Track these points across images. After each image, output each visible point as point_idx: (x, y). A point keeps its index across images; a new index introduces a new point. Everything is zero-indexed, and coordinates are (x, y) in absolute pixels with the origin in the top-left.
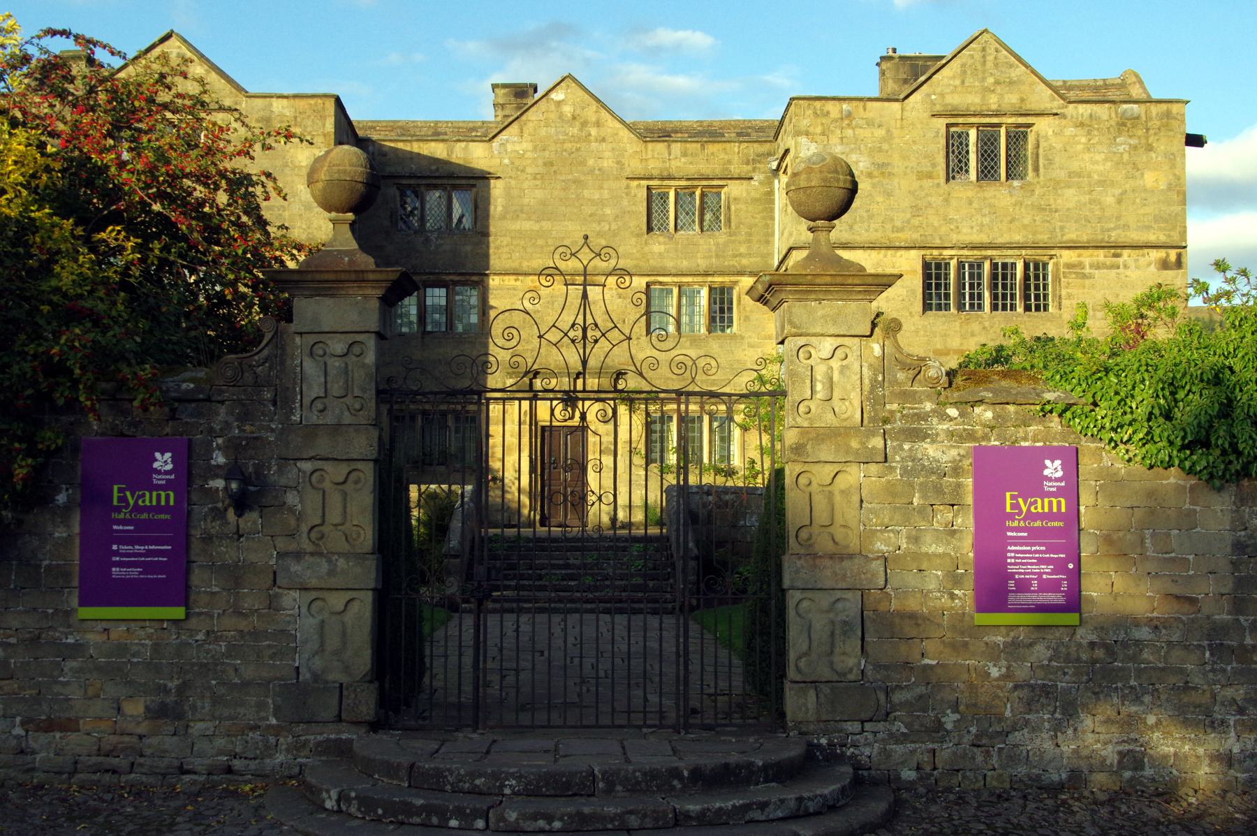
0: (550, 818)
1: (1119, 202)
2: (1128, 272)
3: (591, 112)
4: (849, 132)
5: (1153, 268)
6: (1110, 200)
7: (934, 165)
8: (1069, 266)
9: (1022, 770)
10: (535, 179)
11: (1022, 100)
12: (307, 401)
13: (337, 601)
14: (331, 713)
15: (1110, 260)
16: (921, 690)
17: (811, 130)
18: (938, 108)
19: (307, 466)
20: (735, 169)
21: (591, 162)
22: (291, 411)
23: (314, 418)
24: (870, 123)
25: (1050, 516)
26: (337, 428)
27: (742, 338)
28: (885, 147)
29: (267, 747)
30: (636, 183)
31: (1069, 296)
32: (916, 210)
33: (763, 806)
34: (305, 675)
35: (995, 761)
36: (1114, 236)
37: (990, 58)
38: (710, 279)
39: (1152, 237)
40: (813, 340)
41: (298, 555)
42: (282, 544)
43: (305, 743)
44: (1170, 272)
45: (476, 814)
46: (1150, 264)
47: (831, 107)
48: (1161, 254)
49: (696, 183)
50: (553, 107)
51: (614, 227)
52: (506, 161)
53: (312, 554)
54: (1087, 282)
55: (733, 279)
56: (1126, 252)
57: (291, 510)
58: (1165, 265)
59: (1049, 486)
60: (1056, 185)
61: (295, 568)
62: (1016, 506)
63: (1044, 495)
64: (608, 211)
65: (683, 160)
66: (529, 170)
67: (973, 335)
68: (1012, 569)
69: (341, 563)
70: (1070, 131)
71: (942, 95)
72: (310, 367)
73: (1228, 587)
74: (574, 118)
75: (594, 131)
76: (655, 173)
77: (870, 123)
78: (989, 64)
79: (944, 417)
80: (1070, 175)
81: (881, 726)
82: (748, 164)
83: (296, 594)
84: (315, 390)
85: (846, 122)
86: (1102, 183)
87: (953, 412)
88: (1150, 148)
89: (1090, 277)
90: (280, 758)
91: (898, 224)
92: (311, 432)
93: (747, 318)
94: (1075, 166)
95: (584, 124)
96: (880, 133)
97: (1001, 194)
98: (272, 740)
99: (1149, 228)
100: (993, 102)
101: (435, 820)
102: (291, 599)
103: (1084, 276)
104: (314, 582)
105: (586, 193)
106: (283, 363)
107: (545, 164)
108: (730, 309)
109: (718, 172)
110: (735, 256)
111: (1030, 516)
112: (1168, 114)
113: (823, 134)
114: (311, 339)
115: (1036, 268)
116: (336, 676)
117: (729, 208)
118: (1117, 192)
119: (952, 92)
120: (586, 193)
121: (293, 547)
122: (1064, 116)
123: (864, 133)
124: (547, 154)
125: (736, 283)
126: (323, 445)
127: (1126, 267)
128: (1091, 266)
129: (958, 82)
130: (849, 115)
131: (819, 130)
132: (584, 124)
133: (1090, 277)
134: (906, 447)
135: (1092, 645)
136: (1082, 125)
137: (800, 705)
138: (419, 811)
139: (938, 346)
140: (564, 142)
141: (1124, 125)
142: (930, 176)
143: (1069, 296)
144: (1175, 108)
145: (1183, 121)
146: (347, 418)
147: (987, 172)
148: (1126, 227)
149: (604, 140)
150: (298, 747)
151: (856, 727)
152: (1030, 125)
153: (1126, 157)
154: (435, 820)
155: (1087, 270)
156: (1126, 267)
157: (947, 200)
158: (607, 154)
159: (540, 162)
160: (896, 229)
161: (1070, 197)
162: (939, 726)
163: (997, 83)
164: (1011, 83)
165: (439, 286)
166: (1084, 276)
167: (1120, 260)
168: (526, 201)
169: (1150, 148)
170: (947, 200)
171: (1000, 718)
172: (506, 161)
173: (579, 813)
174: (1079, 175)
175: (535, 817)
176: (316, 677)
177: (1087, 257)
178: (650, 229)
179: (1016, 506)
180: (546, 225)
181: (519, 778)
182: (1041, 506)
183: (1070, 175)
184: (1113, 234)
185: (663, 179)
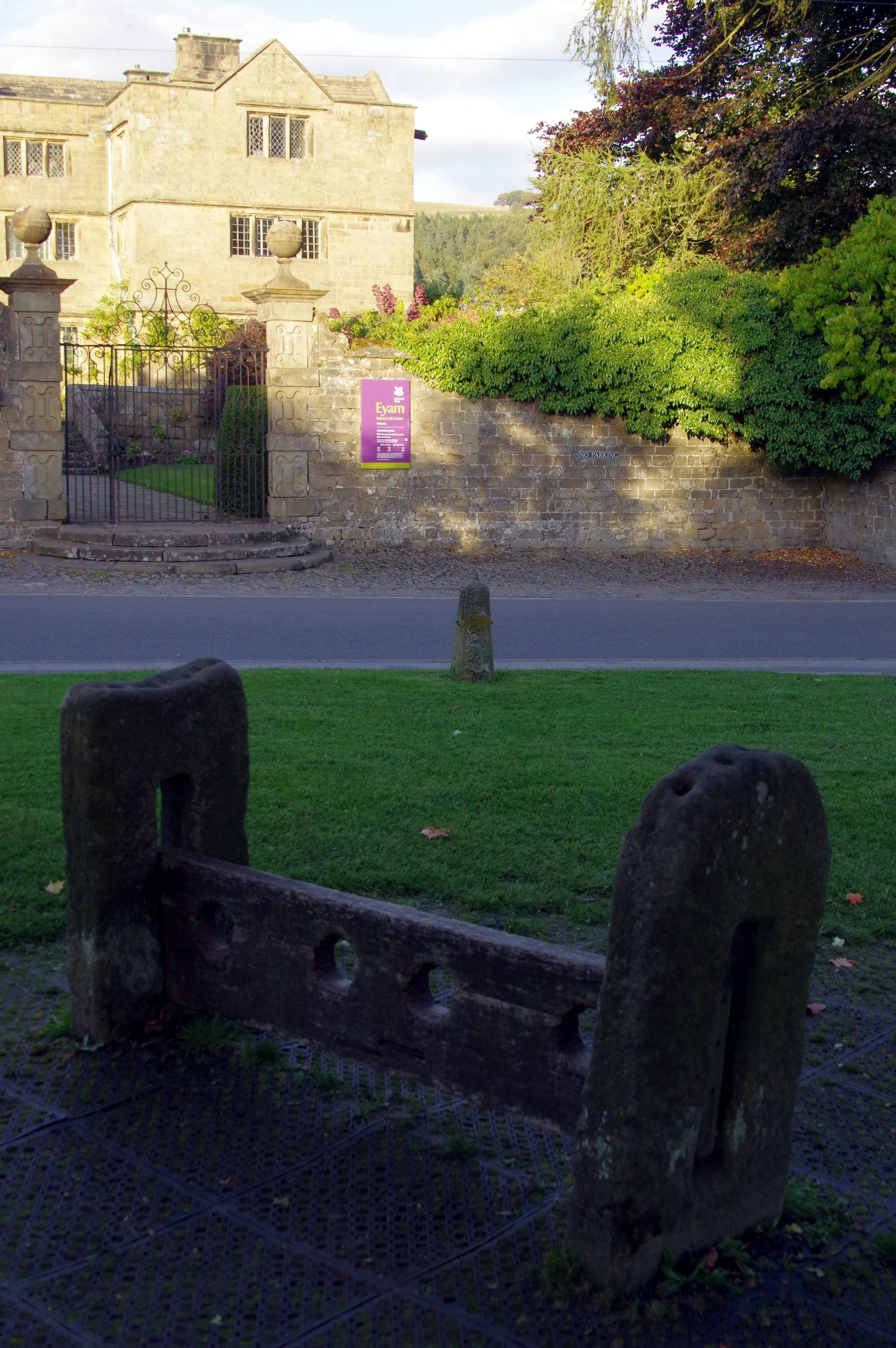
0: (193, 555)
1: (369, 180)
4: (175, 113)
5: (391, 231)
7: (238, 143)
8: (334, 226)
9: (382, 539)
11: (302, 97)
12: (23, 349)
13: (43, 457)
14: (42, 516)
15: (362, 223)
16: (336, 501)
17: (146, 108)
18: (241, 99)
19: (25, 385)
20: (75, 127)
22: (14, 355)
23: (27, 359)
24: (191, 106)
25: (397, 415)
26: (40, 364)
27: (83, 265)
28: (202, 126)
29: (10, 533)
31: (334, 248)
33: (283, 550)
34: (28, 496)
35: (370, 535)
36: (366, 205)
37: (279, 62)
39: (391, 208)
40: (284, 323)
41: (22, 432)
42: (13, 426)
43: (29, 532)
44: (401, 234)
45: (157, 555)
48: (396, 220)
49: (43, 136)
53: (30, 432)
56: (372, 217)
57: (17, 408)
58: (399, 229)
59: (396, 400)
61: (21, 439)
62: (381, 410)
63: (394, 404)
67: (266, 274)
68: (379, 441)
69: (46, 436)
70: (336, 123)
71: (244, 89)
72: (22, 329)
73: (477, 450)
76: (10, 126)
77: (191, 106)
78: (278, 67)
79: (347, 364)
81: (316, 519)
82: (84, 123)
83: (21, 453)
84: (28, 344)
85: (173, 104)
87: (351, 361)
88: (390, 141)
89: (348, 234)
90: (17, 539)
92: (27, 366)
93: (86, 250)
97: (286, 167)
98: (12, 529)
100: (281, 97)
101: (136, 558)
102: (19, 456)
103: (344, 234)
104: (31, 447)
106: (8, 328)
108: (73, 241)
109: (61, 128)
110: (76, 198)
111: (388, 415)
112: (403, 116)
113: (156, 112)
114: (24, 315)
115: (311, 226)
116: (44, 496)
121: (18, 428)
122: (331, 112)
125: (77, 220)
126: (33, 374)
127: (372, 228)
129: (255, 79)
130: (175, 99)
131: (152, 109)
133: (348, 234)
134: (329, 379)
135: (415, 478)
136: (343, 119)
137: (275, 508)
138: (127, 555)
141: (373, 121)
142: (235, 151)
143: (334, 248)
144: (408, 111)
145: (413, 122)
146: (45, 359)
147: (276, 151)
150: (26, 533)
151: (305, 519)
152: (307, 117)
153: (374, 146)
154: (136, 558)
155: (346, 230)
156: (372, 228)
157: (247, 171)
162: (344, 519)
163: (284, 82)
164: (294, 83)
166: (344, 234)
167: (369, 223)
169: (390, 141)
170: (247, 171)
171: (373, 514)
173: (206, 553)
175: (186, 555)
176: (34, 497)
177: (346, 220)
178: (6, 172)
179: (381, 410)
181: (172, 538)
182: (393, 410)
184: (364, 203)
185: (16, 131)
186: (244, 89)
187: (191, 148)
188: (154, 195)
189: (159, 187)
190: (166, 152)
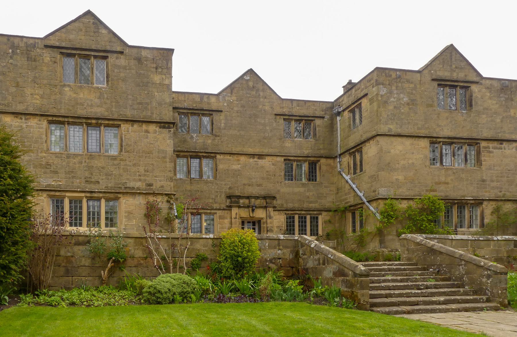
1: (502, 121)
2: (506, 151)
4: (400, 85)
6: (498, 120)
7: (433, 102)
8: (485, 148)
10: (237, 113)
11: (466, 76)
15: (499, 146)
17: (385, 82)
18: (434, 77)
21: (260, 107)
24: (408, 81)
28: (414, 92)
30: (278, 117)
36: (500, 136)
37: (453, 57)
38: (309, 159)
46: (513, 148)
49: (303, 118)
50: (244, 82)
51: (270, 135)
52: (225, 104)
54: (491, 154)
55: (318, 159)
56: (504, 143)
64: (268, 128)
65: (297, 108)
66: (235, 109)
71: (436, 71)
74: (253, 87)
75: (261, 94)
77: (408, 81)
78: (453, 60)
80: (484, 109)
86: (496, 113)
91: (420, 126)
95: (258, 90)
96: (412, 86)
99: (512, 133)
103: (490, 152)
105: (258, 120)
107: (241, 106)
113: (389, 85)
117: (315, 129)
119: (439, 70)
120: (258, 120)
122: (481, 84)
124: (242, 102)
125: (319, 161)
127: (505, 149)
128: (492, 148)
129: (441, 66)
130: (400, 77)
131: (387, 83)
132: (258, 90)
136: (488, 88)
139: (437, 181)
140: (249, 97)
141: (503, 89)
142: (432, 106)
143: (485, 160)
149: (265, 98)
153: (504, 102)
155: (491, 150)
156: (505, 149)
157: (438, 117)
158: (267, 104)
159: (240, 105)
160: (419, 128)
164: (461, 68)
165: (196, 158)
166: (490, 152)
167: (503, 146)
168: (234, 121)
172: (225, 104)
177: (491, 145)
180: (243, 133)
183: (484, 109)
186: (436, 71)
188: (389, 131)
189: (391, 127)
190: (395, 107)
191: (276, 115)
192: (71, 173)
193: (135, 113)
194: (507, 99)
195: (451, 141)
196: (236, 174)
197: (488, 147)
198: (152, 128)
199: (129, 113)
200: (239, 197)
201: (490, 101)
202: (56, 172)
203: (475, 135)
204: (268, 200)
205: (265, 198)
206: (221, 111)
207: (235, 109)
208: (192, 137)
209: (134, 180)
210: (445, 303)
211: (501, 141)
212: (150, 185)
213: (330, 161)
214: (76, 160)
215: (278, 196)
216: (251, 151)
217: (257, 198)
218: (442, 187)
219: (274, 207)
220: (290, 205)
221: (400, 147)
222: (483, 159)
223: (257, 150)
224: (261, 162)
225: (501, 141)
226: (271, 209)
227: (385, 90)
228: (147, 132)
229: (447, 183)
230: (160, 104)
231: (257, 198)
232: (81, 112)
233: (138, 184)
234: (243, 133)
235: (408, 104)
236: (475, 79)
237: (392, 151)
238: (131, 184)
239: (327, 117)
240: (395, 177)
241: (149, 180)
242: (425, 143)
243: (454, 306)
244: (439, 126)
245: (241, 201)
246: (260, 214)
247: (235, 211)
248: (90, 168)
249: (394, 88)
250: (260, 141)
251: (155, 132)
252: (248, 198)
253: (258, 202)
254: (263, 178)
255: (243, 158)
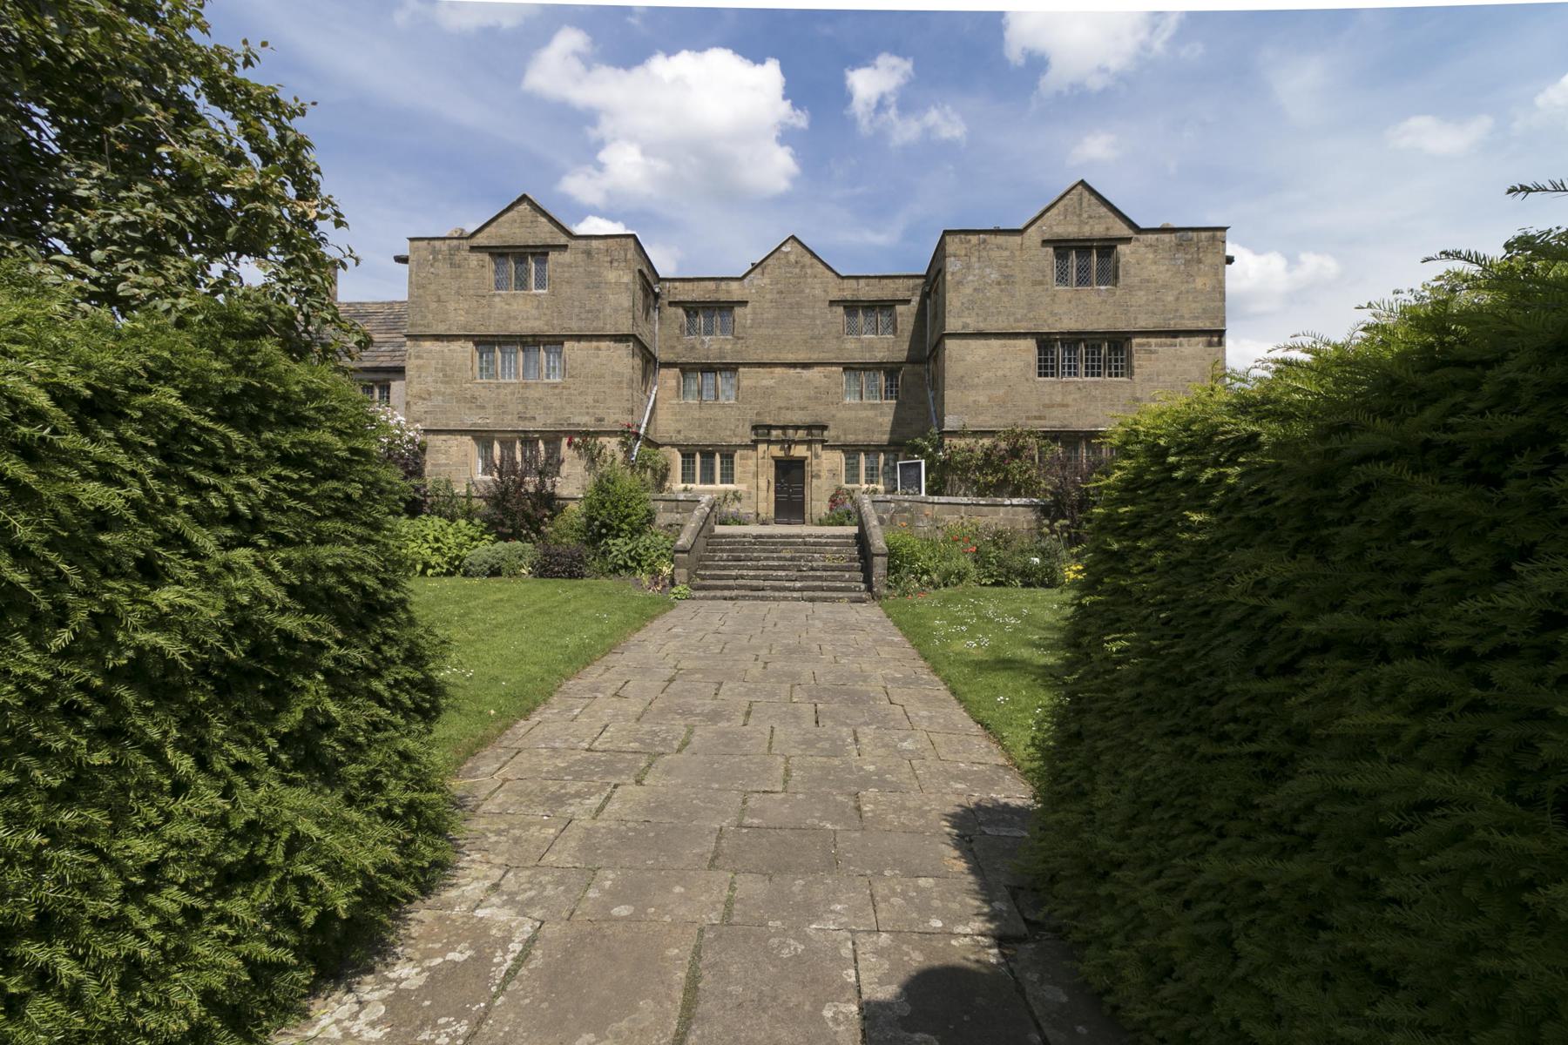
1: (1177, 299)
3: (807, 259)
4: (984, 254)
6: (1170, 298)
8: (1139, 345)
24: (999, 247)
31: (1140, 366)
32: (1031, 306)
36: (1173, 325)
47: (974, 239)
58: (1210, 344)
60: (1130, 289)
70: (1143, 250)
77: (999, 247)
86: (1164, 286)
88: (1199, 261)
94: (1145, 275)
96: (1007, 253)
99: (1197, 318)
103: (1151, 352)
112: (1214, 238)
118: (1176, 292)
123: (995, 254)
142: (1041, 283)
143: (1140, 366)
144: (1219, 234)
148: (1182, 317)
160: (1017, 321)
161: (1141, 297)
166: (1151, 352)
169: (1199, 261)
174: (1148, 281)
177: (1153, 341)
180: (779, 332)
187: (999, 283)
191: (832, 303)
192: (501, 407)
193: (583, 324)
194: (1187, 263)
195: (1072, 340)
196: (767, 392)
197: (1149, 344)
198: (604, 344)
199: (575, 327)
200: (770, 427)
201: (1154, 268)
202: (483, 407)
203: (1122, 326)
204: (815, 431)
205: (809, 428)
206: (746, 302)
207: (768, 296)
208: (703, 342)
209: (580, 414)
210: (800, 590)
211: (1175, 334)
212: (601, 420)
213: (918, 368)
214: (508, 390)
215: (831, 424)
216: (791, 358)
217: (797, 428)
218: (1057, 412)
219: (823, 441)
220: (851, 439)
221: (983, 352)
222: (1135, 363)
223: (802, 357)
224: (806, 373)
225: (1175, 334)
226: (819, 447)
227: (959, 264)
228: (598, 349)
229: (1067, 406)
230: (616, 310)
231: (797, 428)
232: (515, 328)
233: (585, 419)
234: (779, 332)
235: (999, 283)
236: (1126, 232)
237: (968, 358)
238: (576, 420)
239: (916, 300)
240: (971, 399)
241: (600, 413)
242: (1031, 344)
243: (727, 593)
244: (1053, 314)
245: (774, 433)
246: (799, 451)
247: (762, 447)
248: (524, 400)
249: (974, 259)
250: (806, 342)
251: (609, 348)
252: (784, 428)
253: (801, 434)
254: (809, 398)
255: (778, 370)
